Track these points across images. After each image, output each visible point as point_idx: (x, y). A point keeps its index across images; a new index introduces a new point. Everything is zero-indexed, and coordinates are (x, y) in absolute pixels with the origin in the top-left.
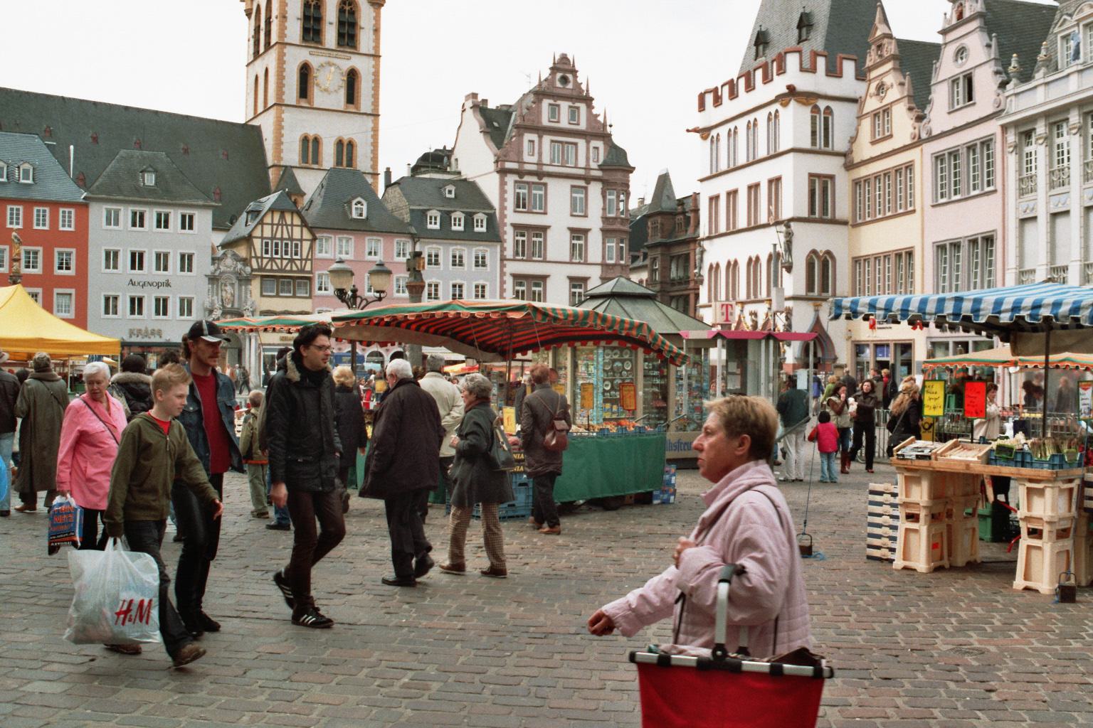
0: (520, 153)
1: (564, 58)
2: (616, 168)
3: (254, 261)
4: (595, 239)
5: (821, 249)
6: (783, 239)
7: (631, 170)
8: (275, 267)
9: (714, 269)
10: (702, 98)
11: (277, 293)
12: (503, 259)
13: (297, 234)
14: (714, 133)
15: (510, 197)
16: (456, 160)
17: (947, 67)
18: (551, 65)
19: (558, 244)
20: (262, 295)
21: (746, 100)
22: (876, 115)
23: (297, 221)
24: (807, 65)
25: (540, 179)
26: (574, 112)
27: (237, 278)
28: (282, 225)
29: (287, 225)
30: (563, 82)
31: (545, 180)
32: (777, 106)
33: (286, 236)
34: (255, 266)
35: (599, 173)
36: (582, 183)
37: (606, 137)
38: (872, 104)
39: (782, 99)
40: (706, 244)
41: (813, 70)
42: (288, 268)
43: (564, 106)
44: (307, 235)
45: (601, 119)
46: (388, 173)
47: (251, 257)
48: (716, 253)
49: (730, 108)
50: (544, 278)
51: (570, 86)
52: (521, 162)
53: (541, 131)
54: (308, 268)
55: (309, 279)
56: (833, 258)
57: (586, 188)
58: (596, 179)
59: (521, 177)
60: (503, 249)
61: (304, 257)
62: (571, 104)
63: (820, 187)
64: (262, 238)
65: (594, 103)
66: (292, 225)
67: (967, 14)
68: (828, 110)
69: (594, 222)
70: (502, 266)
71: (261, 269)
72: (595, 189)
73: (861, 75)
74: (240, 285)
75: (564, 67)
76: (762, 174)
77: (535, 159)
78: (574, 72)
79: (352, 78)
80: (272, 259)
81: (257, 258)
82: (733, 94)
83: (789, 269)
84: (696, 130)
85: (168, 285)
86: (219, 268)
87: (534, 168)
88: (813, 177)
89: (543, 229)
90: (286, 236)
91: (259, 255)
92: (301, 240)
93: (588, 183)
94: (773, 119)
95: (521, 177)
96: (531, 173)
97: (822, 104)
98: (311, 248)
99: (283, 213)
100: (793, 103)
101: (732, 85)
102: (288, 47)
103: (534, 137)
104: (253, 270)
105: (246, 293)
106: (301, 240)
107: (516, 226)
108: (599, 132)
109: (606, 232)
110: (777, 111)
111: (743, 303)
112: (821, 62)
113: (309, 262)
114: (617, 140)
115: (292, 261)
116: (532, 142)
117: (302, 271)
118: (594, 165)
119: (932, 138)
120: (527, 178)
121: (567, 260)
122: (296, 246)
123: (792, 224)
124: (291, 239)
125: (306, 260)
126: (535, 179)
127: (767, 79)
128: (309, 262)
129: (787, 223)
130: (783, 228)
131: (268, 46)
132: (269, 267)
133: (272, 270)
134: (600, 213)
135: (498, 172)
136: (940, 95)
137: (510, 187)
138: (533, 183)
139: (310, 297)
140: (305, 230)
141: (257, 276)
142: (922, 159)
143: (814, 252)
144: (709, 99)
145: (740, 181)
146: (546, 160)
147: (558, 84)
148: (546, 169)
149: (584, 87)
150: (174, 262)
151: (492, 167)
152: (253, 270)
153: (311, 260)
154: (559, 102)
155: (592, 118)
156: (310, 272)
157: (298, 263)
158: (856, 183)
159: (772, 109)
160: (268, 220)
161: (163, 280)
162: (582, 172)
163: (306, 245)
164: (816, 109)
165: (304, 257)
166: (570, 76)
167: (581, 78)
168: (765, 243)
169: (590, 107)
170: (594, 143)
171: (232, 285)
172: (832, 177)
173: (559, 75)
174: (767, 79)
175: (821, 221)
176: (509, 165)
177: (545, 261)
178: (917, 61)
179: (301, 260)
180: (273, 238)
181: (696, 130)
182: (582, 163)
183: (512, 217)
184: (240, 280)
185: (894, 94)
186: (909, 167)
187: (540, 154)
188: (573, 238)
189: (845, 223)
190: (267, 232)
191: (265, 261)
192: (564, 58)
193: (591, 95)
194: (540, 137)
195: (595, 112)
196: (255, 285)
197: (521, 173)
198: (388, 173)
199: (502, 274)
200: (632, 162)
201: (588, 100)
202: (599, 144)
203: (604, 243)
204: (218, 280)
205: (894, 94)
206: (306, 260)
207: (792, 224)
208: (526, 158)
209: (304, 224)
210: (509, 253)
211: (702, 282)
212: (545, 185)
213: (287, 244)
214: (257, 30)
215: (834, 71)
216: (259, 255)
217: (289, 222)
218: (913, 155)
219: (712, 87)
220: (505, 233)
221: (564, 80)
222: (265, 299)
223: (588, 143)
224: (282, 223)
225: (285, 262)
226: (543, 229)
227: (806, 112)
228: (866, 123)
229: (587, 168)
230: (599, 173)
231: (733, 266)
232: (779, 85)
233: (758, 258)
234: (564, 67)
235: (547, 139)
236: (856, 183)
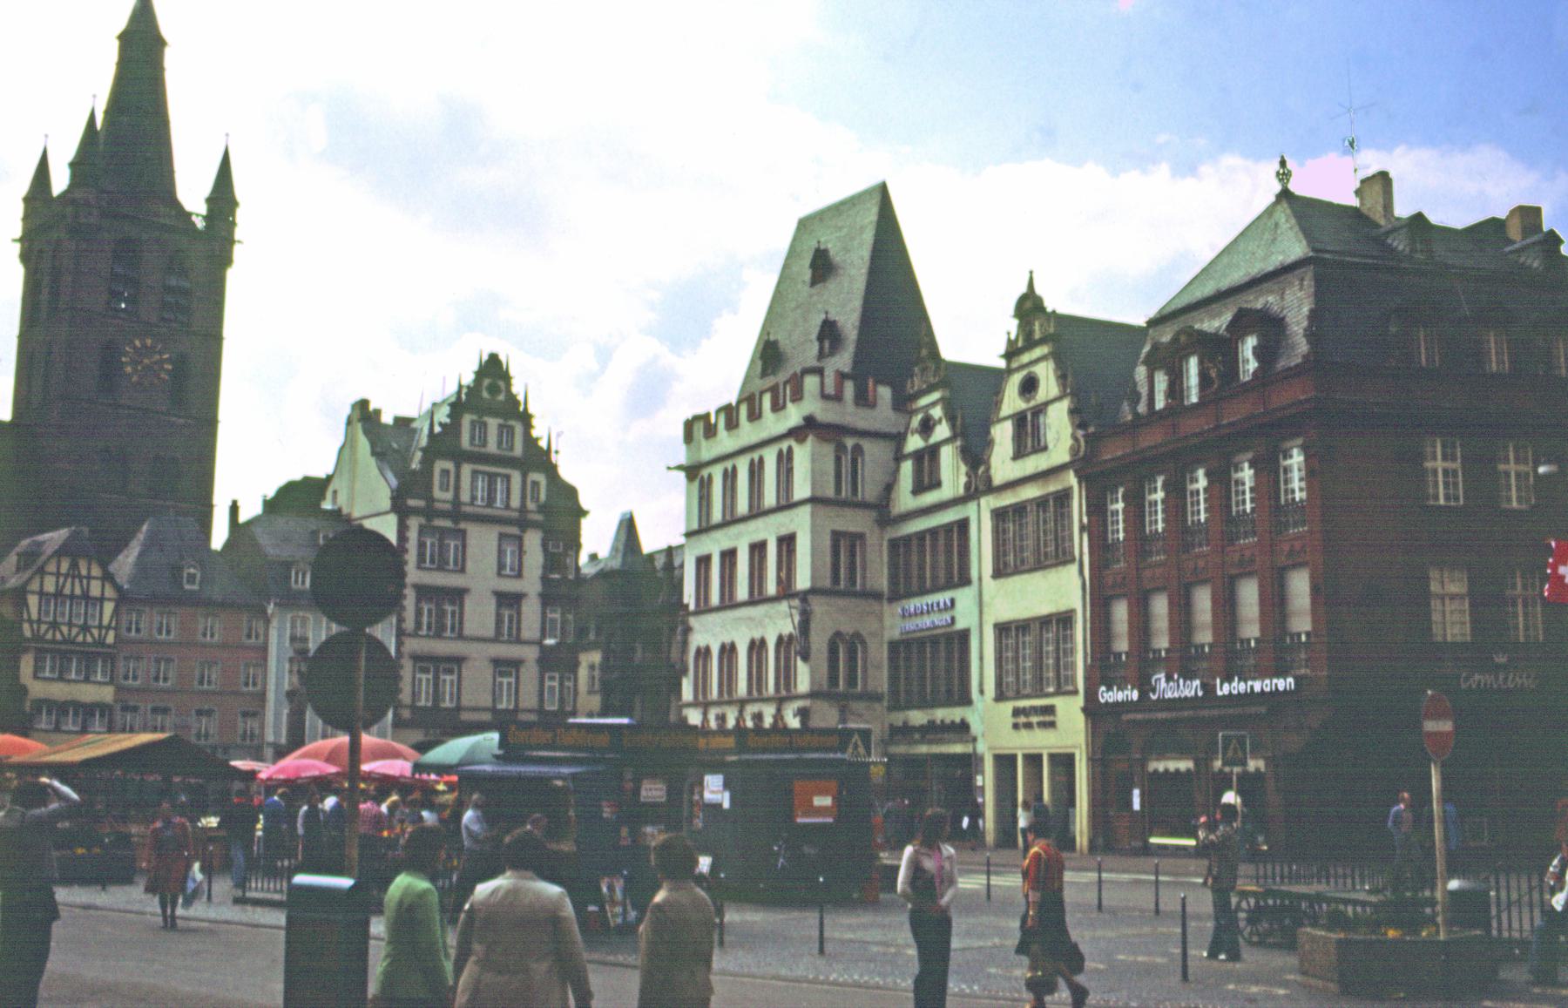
0: (429, 487)
1: (494, 359)
2: (563, 510)
3: (26, 626)
4: (531, 611)
5: (847, 628)
6: (797, 619)
7: (584, 513)
9: (704, 653)
10: (689, 426)
13: (95, 590)
14: (705, 473)
15: (412, 546)
16: (335, 492)
17: (1012, 402)
18: (476, 368)
19: (479, 615)
20: (36, 677)
21: (748, 433)
22: (918, 456)
24: (830, 389)
25: (456, 522)
26: (506, 432)
28: (73, 577)
29: (81, 578)
30: (491, 391)
31: (462, 526)
32: (792, 442)
33: (78, 591)
34: (28, 633)
35: (539, 517)
36: (514, 530)
37: (551, 470)
38: (914, 443)
39: (796, 433)
40: (693, 621)
41: (838, 397)
43: (493, 423)
45: (543, 444)
46: (234, 509)
47: (22, 621)
48: (707, 633)
49: (726, 442)
50: (459, 660)
51: (501, 397)
52: (430, 499)
53: (460, 457)
56: (863, 642)
57: (520, 539)
58: (535, 525)
59: (429, 519)
60: (401, 620)
61: (106, 621)
62: (501, 421)
63: (844, 547)
64: (41, 593)
65: (534, 422)
66: (89, 577)
67: (1037, 335)
68: (858, 450)
69: (531, 584)
71: (37, 638)
72: (533, 540)
73: (903, 403)
75: (493, 370)
76: (767, 530)
77: (449, 496)
78: (506, 377)
79: (181, 362)
80: (54, 625)
81: (30, 621)
82: (732, 425)
83: (805, 658)
84: (679, 468)
87: (448, 506)
88: (837, 536)
89: (457, 595)
90: (78, 591)
91: (34, 616)
92: (102, 599)
93: (523, 531)
94: (785, 460)
95: (429, 519)
96: (443, 514)
97: (850, 442)
98: (116, 612)
100: (810, 439)
101: (729, 412)
103: (449, 465)
108: (539, 459)
109: (547, 600)
110: (790, 450)
111: (742, 703)
112: (849, 389)
114: (567, 473)
115: (85, 628)
116: (445, 472)
117: (101, 642)
118: (531, 506)
119: (990, 489)
121: (491, 633)
123: (810, 597)
124: (86, 596)
125: (108, 628)
126: (448, 524)
127: (777, 407)
129: (804, 596)
130: (796, 602)
132: (49, 636)
133: (54, 641)
134: (539, 572)
136: (1003, 434)
137: (413, 535)
142: (981, 518)
143: (838, 634)
144: (699, 429)
145: (740, 539)
146: (465, 496)
147: (485, 394)
148: (468, 509)
149: (521, 398)
151: (386, 504)
154: (486, 419)
155: (530, 442)
157: (95, 632)
158: (894, 544)
159: (784, 445)
160: (52, 568)
162: (515, 515)
163: (109, 608)
164: (840, 449)
165: (106, 621)
166: (502, 384)
167: (514, 390)
168: (778, 622)
172: (861, 536)
173: (486, 382)
174: (777, 407)
175: (849, 594)
176: (412, 503)
177: (461, 637)
178: (971, 394)
179: (100, 627)
180: (58, 594)
181: (679, 468)
182: (515, 502)
183: (413, 575)
185: (942, 431)
186: (963, 525)
187: (457, 488)
188: (499, 605)
189: (877, 596)
190: (50, 585)
191: (44, 627)
192: (494, 359)
193: (531, 410)
194: (458, 468)
195: (535, 433)
197: (430, 512)
198: (234, 509)
200: (584, 501)
201: (526, 419)
202: (540, 478)
203: (544, 614)
205: (942, 431)
206: (108, 628)
207: (810, 597)
208: (437, 493)
210: (409, 624)
211: (685, 671)
212: (463, 533)
215: (864, 399)
216: (34, 616)
217: (84, 572)
218: (970, 510)
219: (701, 411)
220: (405, 597)
221: (494, 390)
223: (524, 476)
224: (74, 573)
225: (75, 631)
226: (458, 595)
227: (828, 450)
228: (907, 468)
230: (539, 517)
231: (728, 651)
232: (793, 416)
233: (763, 642)
234: (493, 370)
235: (467, 470)
236: (894, 544)
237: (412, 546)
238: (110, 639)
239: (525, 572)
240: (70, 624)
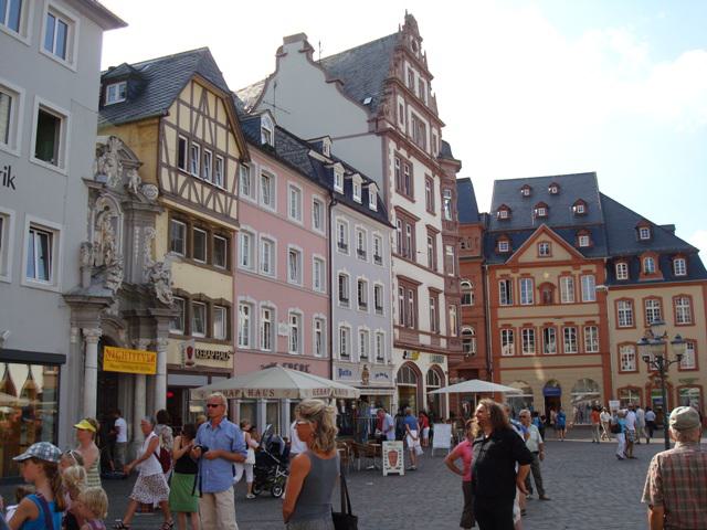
8: (194, 199)
13: (221, 146)
23: (222, 119)
27: (124, 204)
31: (412, 160)
33: (208, 140)
34: (167, 187)
44: (233, 151)
52: (396, 125)
54: (233, 215)
64: (177, 128)
66: (217, 123)
69: (437, 224)
71: (175, 195)
74: (129, 224)
81: (168, 167)
99: (205, 90)
104: (161, 193)
105: (142, 242)
117: (226, 216)
122: (217, 162)
133: (188, 202)
135: (378, 134)
140: (230, 134)
141: (164, 206)
146: (411, 134)
151: (365, 128)
152: (161, 193)
156: (236, 222)
160: (185, 96)
183: (396, 200)
194: (406, 103)
208: (400, 126)
217: (212, 116)
223: (431, 127)
229: (432, 157)
237: (392, 168)
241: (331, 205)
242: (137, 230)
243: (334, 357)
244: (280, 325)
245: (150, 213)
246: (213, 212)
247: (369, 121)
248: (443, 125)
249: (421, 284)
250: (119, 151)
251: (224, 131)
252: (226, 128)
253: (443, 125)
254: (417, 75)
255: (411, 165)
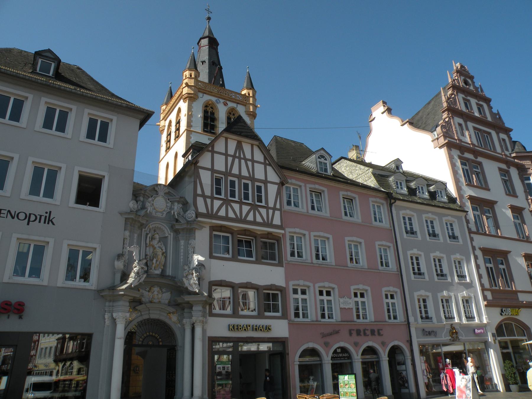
3: (200, 201)
8: (231, 215)
11: (233, 256)
12: (470, 232)
13: (259, 173)
23: (259, 156)
26: (480, 108)
27: (172, 227)
28: (240, 159)
29: (246, 160)
31: (480, 159)
33: (245, 173)
34: (202, 209)
36: (504, 166)
42: (250, 218)
44: (273, 176)
47: (196, 195)
54: (277, 221)
55: (278, 239)
61: (271, 205)
64: (213, 170)
66: (253, 161)
70: (472, 240)
74: (176, 240)
81: (203, 196)
85: (49, 220)
86: (143, 207)
91: (208, 193)
98: (279, 193)
102: (193, 133)
106: (266, 182)
107: (472, 199)
113: (277, 213)
120: (467, 155)
122: (259, 188)
124: (252, 179)
125: (274, 209)
128: (277, 213)
131: (177, 137)
132: (222, 213)
138: (473, 161)
139: (280, 264)
140: (269, 168)
150: (67, 187)
152: (198, 214)
153: (280, 210)
161: (41, 211)
163: (272, 190)
165: (271, 205)
167: (477, 85)
169: (490, 108)
170: (503, 136)
171: (164, 240)
179: (267, 208)
180: (228, 173)
184: (176, 232)
191: (217, 204)
194: (465, 122)
195: (494, 111)
196: (202, 237)
199: (474, 248)
204: (142, 226)
206: (274, 209)
209: (268, 161)
213: (246, 186)
214: (169, 135)
216: (208, 193)
217: (248, 156)
222: (213, 261)
223: (498, 134)
225: (246, 209)
238: (277, 221)
239: (518, 194)
240: (241, 203)
241: (391, 205)
242: (182, 242)
243: (411, 319)
244: (342, 300)
245: (190, 231)
246: (254, 223)
247: (433, 141)
248: (511, 130)
249: (510, 252)
250: (165, 193)
251: (262, 166)
252: (265, 164)
253: (511, 130)
254: (473, 101)
255: (480, 164)
